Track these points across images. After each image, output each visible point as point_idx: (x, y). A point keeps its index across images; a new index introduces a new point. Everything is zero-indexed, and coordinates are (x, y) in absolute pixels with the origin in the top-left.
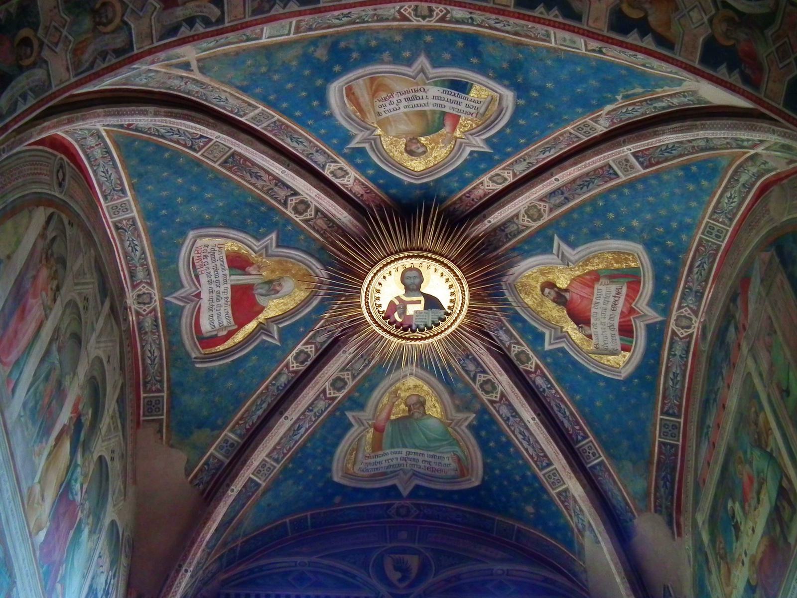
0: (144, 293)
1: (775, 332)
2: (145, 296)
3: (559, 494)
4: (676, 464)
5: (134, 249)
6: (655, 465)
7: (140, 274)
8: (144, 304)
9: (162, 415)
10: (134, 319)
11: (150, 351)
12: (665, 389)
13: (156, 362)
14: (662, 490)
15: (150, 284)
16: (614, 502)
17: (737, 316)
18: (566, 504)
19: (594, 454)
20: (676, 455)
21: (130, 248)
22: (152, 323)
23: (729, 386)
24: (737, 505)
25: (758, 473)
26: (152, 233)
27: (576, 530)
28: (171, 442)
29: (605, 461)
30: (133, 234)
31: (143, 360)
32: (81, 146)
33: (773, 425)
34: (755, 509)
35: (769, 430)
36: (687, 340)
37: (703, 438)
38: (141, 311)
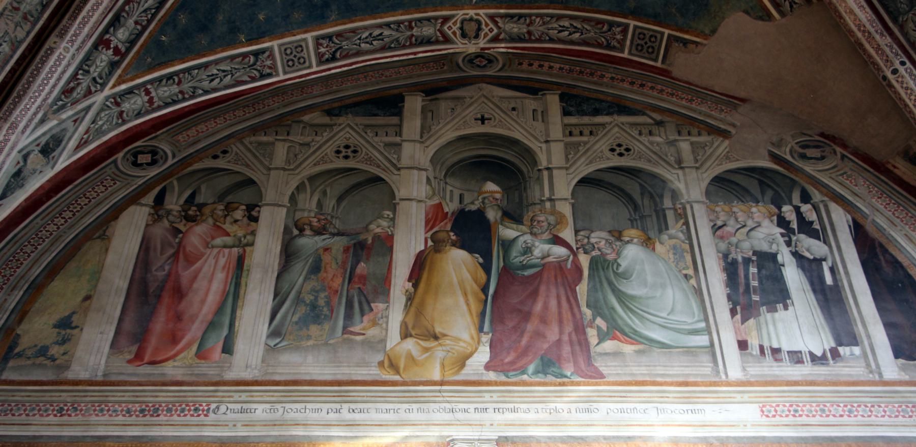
0: (461, 28)
2: (466, 27)
5: (380, 37)
7: (428, 31)
8: (479, 29)
9: (662, 34)
10: (503, 45)
11: (560, 32)
13: (579, 26)
15: (446, 19)
21: (374, 43)
22: (515, 22)
26: (349, 12)
28: (707, 32)
30: (347, 39)
31: (572, 43)
32: (139, 115)
38: (491, 35)
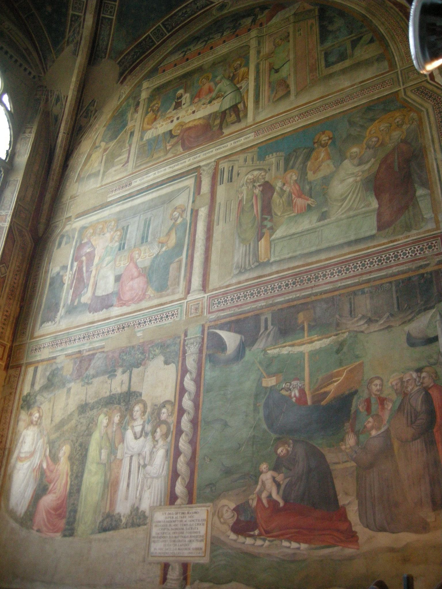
1: (289, 41)
3: (74, 15)
4: (147, 50)
6: (137, 43)
12: (175, 14)
14: (130, 57)
16: (101, 42)
17: (259, 17)
18: (73, 23)
19: (111, 12)
20: (150, 47)
23: (224, 42)
24: (188, 95)
25: (220, 91)
27: (66, 39)
29: (114, 20)
33: (252, 77)
34: (204, 104)
35: (245, 77)
36: (209, 3)
37: (180, 52)
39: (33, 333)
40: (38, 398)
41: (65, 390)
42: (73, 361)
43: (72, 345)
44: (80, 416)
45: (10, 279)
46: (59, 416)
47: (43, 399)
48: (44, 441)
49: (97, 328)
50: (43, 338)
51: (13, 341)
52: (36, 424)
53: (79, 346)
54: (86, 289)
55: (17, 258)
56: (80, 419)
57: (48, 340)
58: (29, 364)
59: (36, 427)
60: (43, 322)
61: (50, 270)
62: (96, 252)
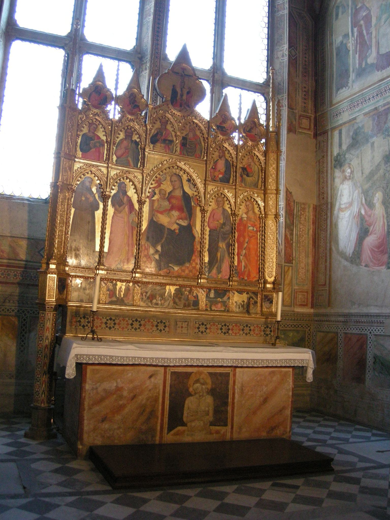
39: (331, 102)
40: (347, 156)
41: (369, 145)
42: (371, 118)
43: (368, 104)
44: (386, 165)
45: (301, 59)
46: (368, 169)
47: (351, 156)
48: (359, 192)
49: (387, 83)
50: (341, 103)
51: (316, 112)
52: (350, 179)
53: (374, 103)
54: (370, 50)
55: (303, 39)
56: (386, 168)
57: (346, 104)
58: (333, 129)
59: (350, 181)
60: (338, 90)
61: (334, 41)
62: (372, 14)
